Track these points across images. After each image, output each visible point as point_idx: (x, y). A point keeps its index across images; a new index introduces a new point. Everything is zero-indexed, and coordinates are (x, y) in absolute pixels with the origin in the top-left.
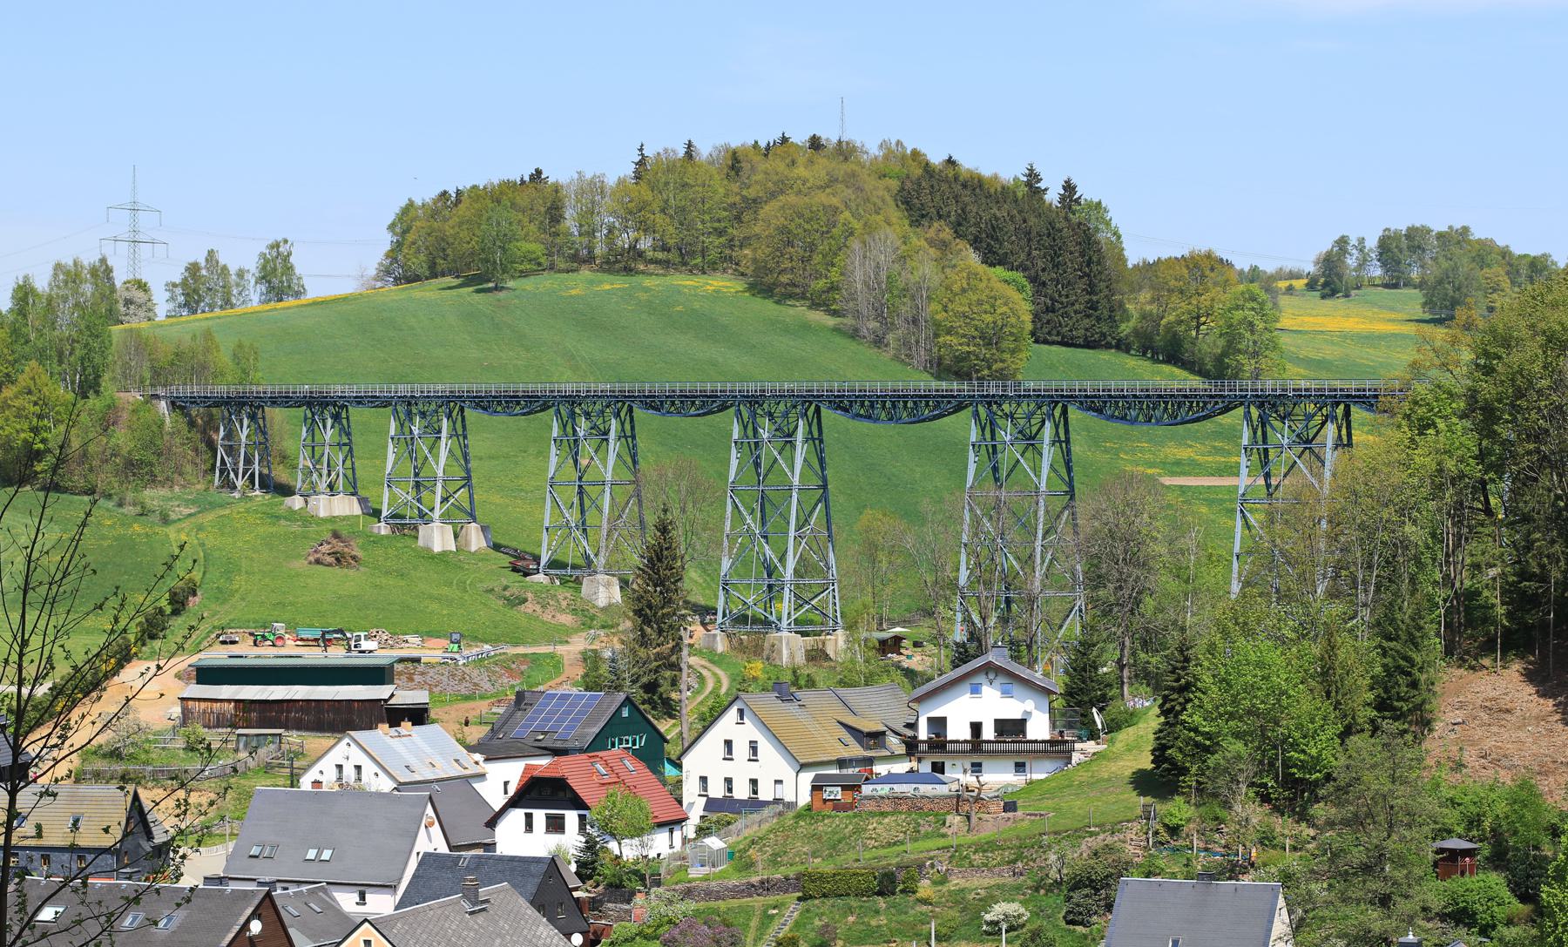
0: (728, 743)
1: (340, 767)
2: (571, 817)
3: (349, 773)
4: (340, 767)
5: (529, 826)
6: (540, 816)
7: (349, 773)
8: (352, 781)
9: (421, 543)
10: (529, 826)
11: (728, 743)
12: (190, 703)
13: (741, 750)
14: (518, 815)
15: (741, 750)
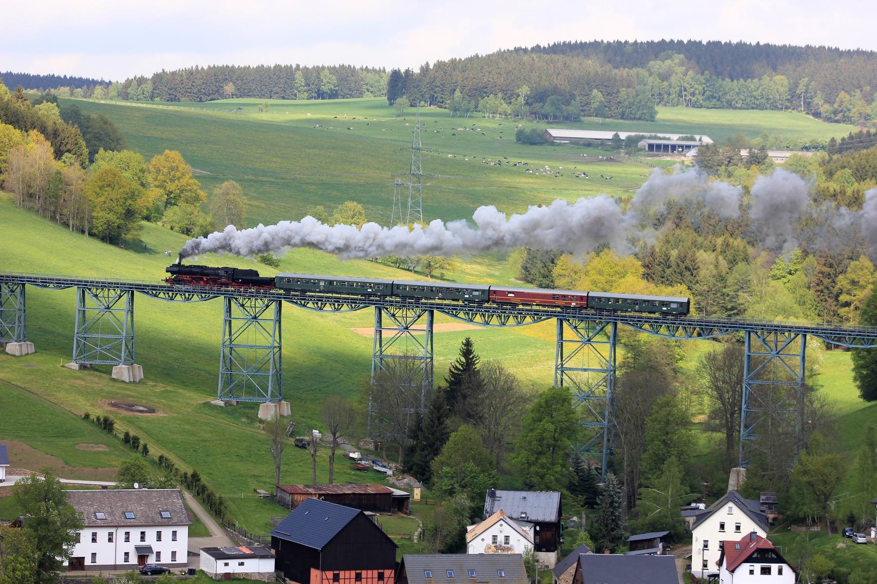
0: (722, 526)
1: (495, 537)
2: (774, 567)
3: (501, 539)
4: (495, 537)
5: (752, 572)
6: (757, 567)
7: (501, 539)
8: (503, 545)
9: (114, 376)
10: (752, 572)
11: (722, 526)
12: (296, 497)
13: (730, 527)
14: (746, 567)
15: (730, 527)
